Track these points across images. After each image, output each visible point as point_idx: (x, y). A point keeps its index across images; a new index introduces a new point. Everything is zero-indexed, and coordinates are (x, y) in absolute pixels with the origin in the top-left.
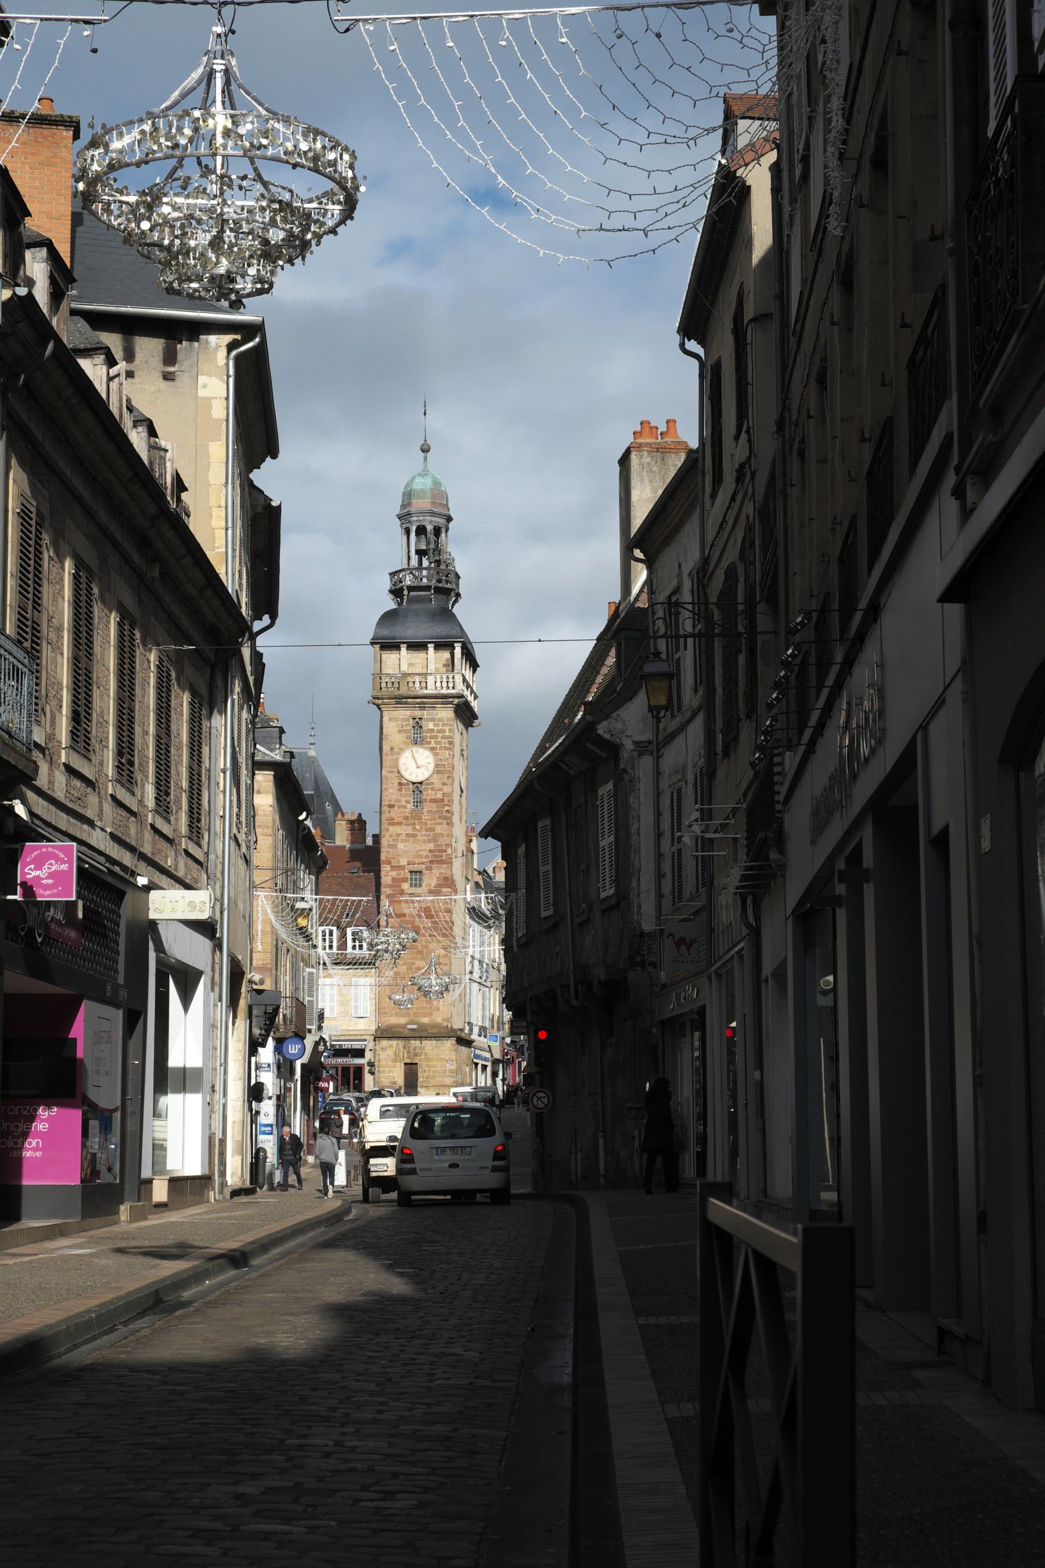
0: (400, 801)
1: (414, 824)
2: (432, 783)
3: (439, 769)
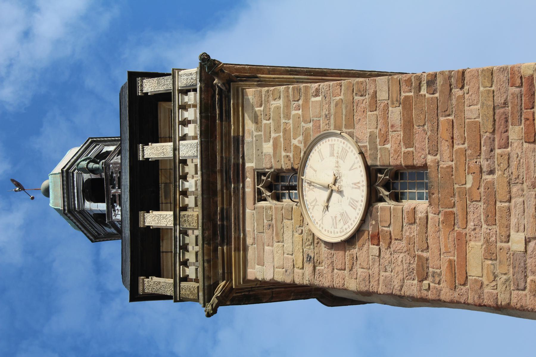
0: (410, 241)
1: (464, 193)
2: (372, 137)
3: (345, 125)
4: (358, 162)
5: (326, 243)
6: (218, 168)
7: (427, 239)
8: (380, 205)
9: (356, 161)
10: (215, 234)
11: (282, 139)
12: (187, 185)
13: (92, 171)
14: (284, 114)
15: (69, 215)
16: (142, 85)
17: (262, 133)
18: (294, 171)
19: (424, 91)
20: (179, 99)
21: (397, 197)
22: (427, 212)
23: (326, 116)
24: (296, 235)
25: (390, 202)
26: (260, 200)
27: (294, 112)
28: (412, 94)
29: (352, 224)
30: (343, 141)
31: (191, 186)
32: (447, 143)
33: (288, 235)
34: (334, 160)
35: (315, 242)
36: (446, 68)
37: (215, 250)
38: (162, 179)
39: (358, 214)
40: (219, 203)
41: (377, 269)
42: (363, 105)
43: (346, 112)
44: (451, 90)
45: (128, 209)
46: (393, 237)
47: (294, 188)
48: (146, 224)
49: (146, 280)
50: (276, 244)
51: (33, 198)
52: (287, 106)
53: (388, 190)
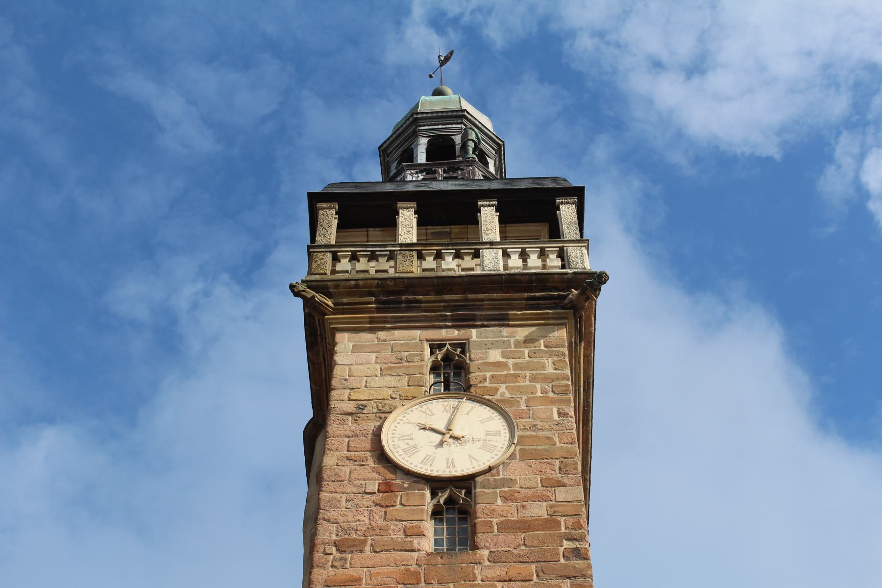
0: (384, 530)
3: (525, 449)
4: (479, 465)
5: (380, 428)
6: (470, 296)
7: (386, 551)
8: (428, 494)
9: (481, 463)
10: (390, 293)
11: (505, 372)
12: (449, 258)
13: (464, 146)
14: (537, 374)
15: (411, 119)
16: (568, 203)
17: (513, 349)
18: (468, 387)
19: (566, 544)
20: (552, 247)
21: (436, 514)
22: (419, 550)
23: (535, 426)
24: (390, 392)
25: (431, 505)
26: (433, 349)
27: (538, 386)
28: (563, 530)
29: (403, 459)
30: (505, 447)
31: (447, 264)
32: (504, 573)
33: (389, 381)
34: (482, 435)
35: (381, 415)
36: (595, 572)
37: (371, 294)
38: (455, 229)
39: (416, 466)
40: (428, 297)
41: (349, 490)
42: (548, 471)
43: (540, 450)
44: (569, 578)
45: (418, 189)
46: (388, 509)
47: (447, 388)
48: (401, 211)
49: (334, 212)
50: (378, 367)
51: (431, 76)
52: (546, 379)
53: (445, 503)
